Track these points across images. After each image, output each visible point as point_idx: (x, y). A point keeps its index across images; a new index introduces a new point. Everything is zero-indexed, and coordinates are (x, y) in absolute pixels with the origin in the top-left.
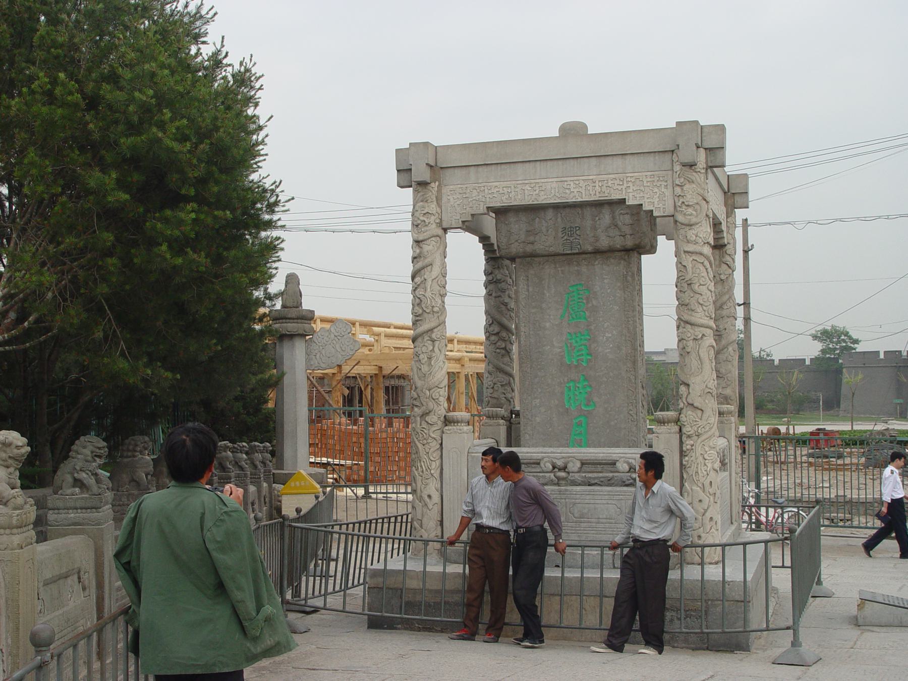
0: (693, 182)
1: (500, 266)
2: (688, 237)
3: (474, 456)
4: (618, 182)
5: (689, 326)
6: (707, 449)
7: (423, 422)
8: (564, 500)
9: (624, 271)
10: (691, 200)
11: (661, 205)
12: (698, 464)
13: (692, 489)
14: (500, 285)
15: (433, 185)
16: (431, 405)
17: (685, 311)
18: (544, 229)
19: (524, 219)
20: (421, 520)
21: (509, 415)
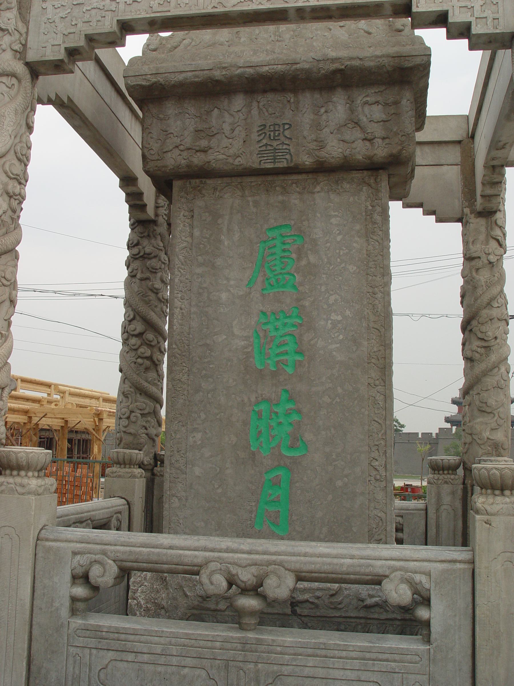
3: (50, 548)
8: (251, 666)
9: (368, 204)
11: (488, 13)
14: (148, 263)
18: (227, 127)
19: (192, 110)
21: (152, 462)
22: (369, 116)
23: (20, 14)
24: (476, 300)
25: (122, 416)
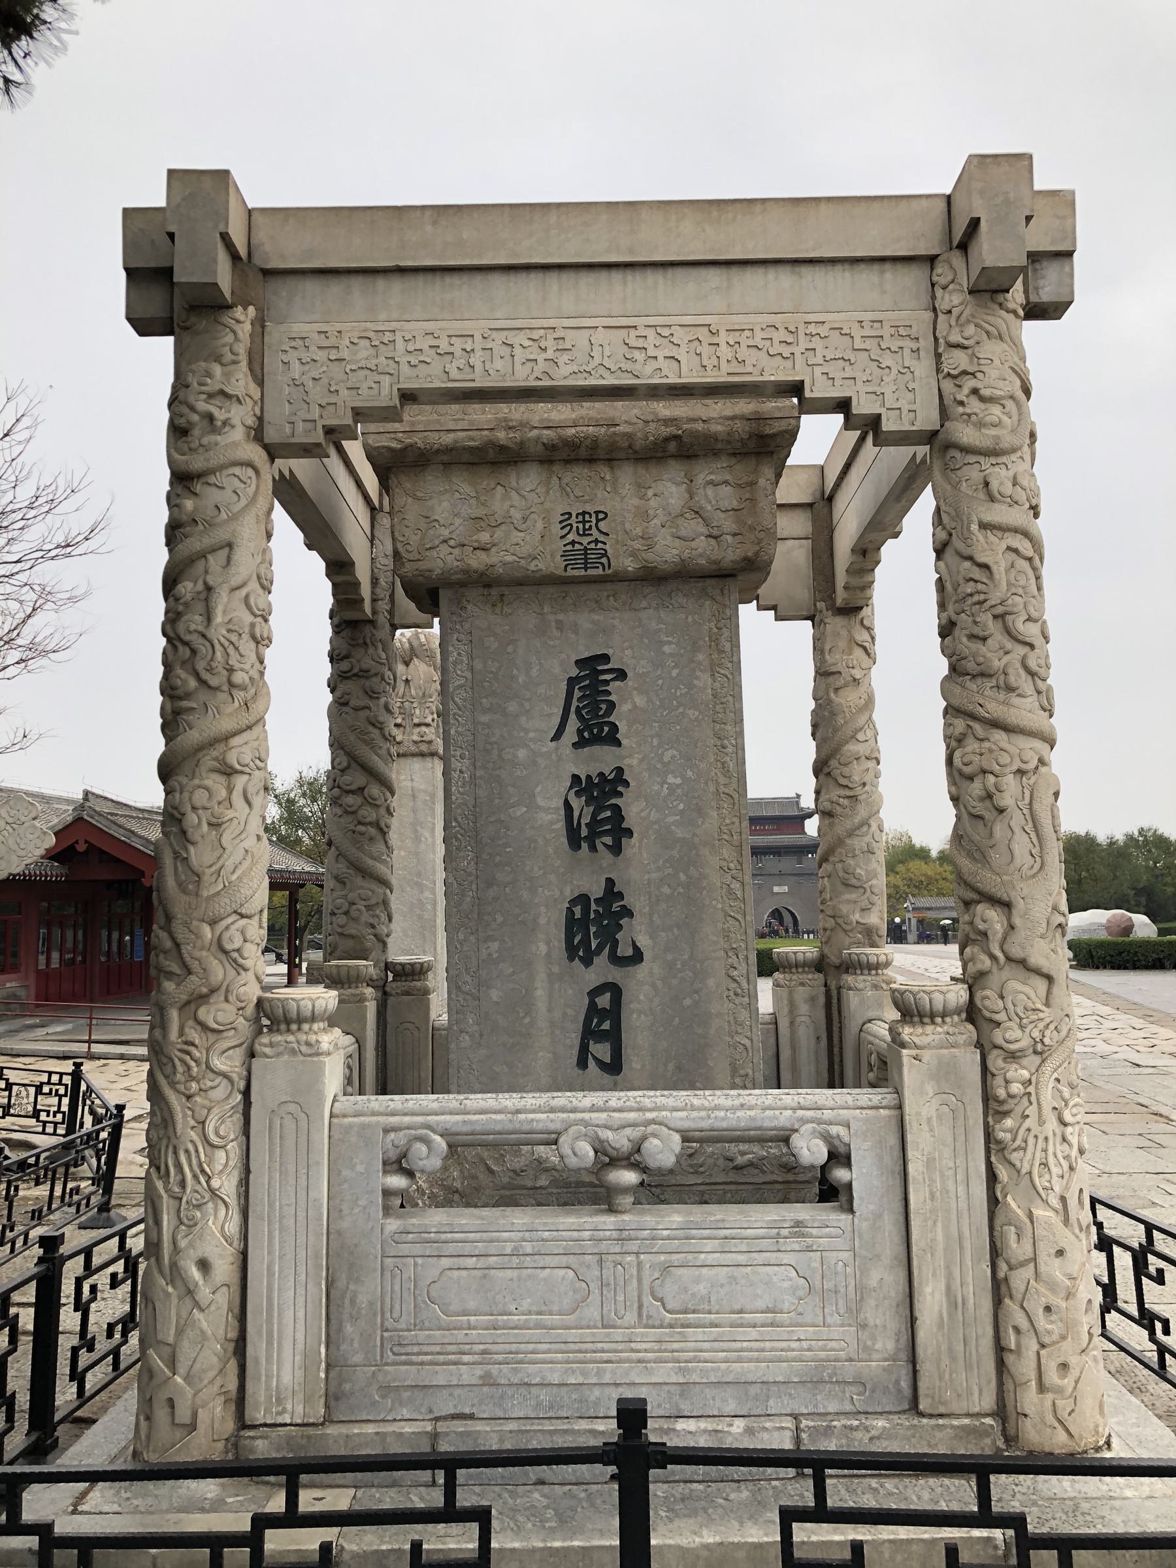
0: (1001, 338)
1: (368, 641)
2: (994, 485)
4: (782, 335)
5: (999, 736)
6: (1066, 1092)
7: (191, 1023)
10: (1001, 384)
12: (1046, 1139)
13: (1030, 1216)
15: (238, 312)
16: (218, 971)
17: (988, 692)
18: (517, 515)
19: (466, 488)
20: (174, 1348)
21: (383, 975)
22: (714, 502)
23: (251, 370)
24: (835, 731)
25: (336, 911)
